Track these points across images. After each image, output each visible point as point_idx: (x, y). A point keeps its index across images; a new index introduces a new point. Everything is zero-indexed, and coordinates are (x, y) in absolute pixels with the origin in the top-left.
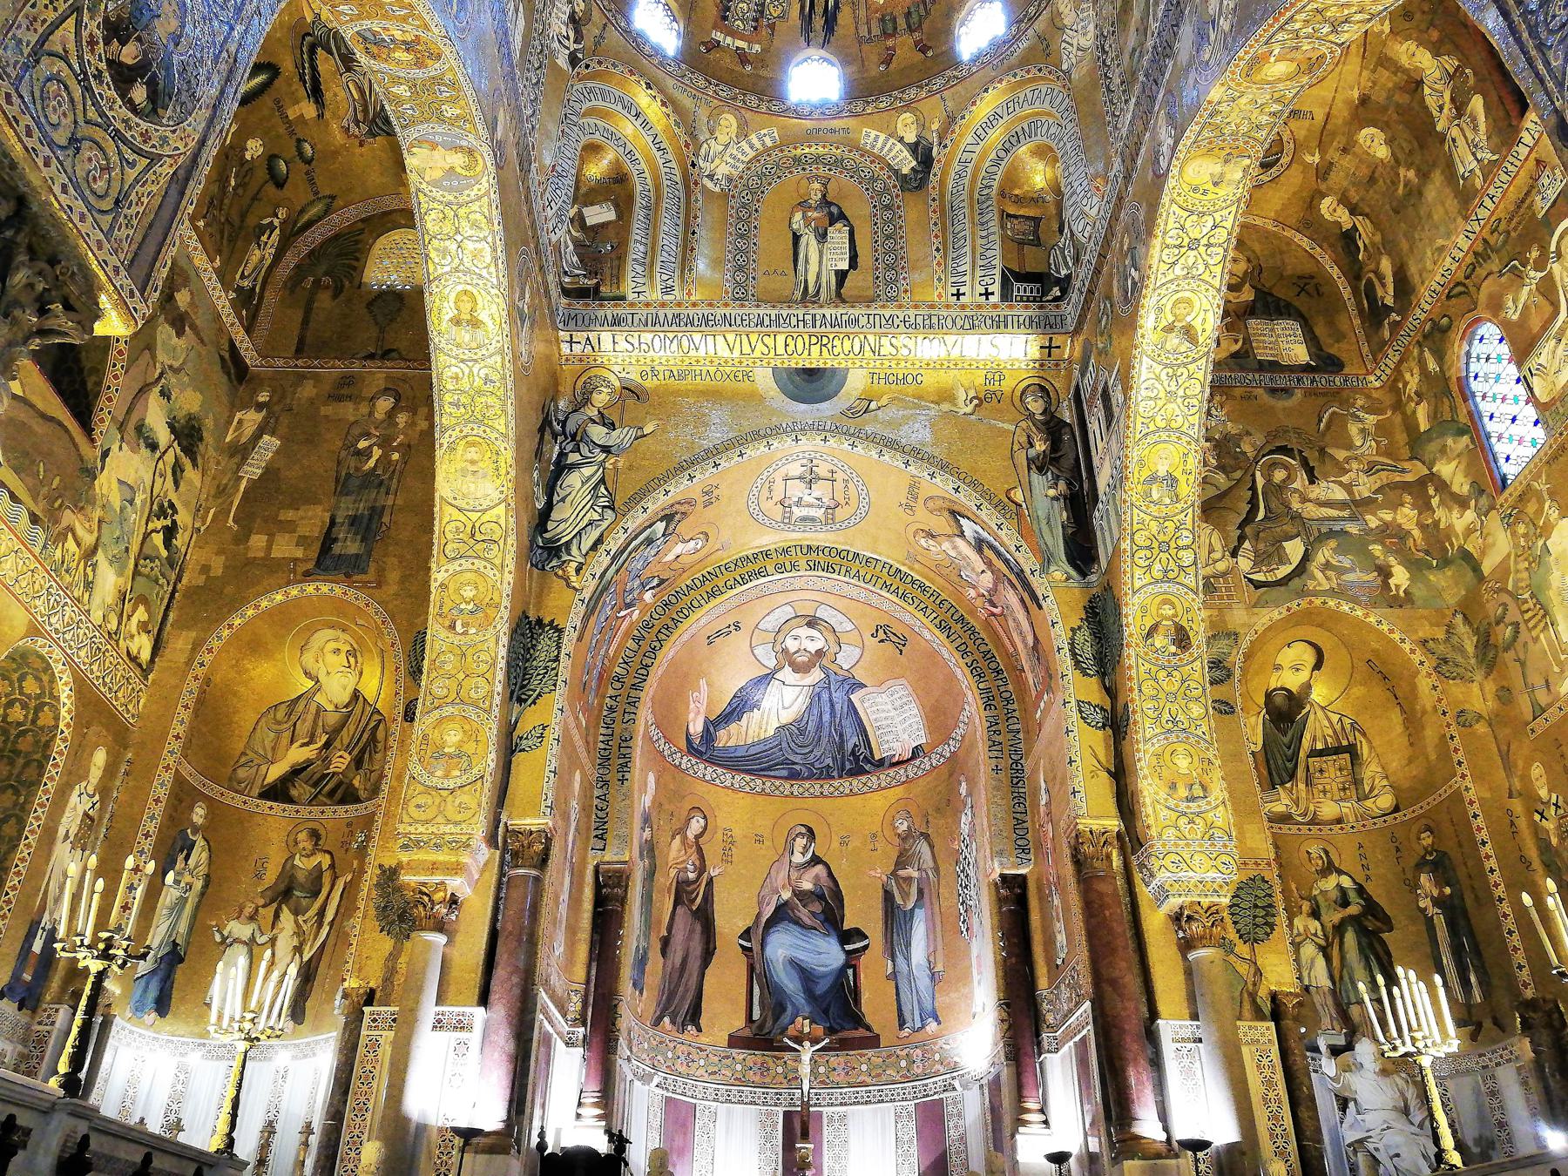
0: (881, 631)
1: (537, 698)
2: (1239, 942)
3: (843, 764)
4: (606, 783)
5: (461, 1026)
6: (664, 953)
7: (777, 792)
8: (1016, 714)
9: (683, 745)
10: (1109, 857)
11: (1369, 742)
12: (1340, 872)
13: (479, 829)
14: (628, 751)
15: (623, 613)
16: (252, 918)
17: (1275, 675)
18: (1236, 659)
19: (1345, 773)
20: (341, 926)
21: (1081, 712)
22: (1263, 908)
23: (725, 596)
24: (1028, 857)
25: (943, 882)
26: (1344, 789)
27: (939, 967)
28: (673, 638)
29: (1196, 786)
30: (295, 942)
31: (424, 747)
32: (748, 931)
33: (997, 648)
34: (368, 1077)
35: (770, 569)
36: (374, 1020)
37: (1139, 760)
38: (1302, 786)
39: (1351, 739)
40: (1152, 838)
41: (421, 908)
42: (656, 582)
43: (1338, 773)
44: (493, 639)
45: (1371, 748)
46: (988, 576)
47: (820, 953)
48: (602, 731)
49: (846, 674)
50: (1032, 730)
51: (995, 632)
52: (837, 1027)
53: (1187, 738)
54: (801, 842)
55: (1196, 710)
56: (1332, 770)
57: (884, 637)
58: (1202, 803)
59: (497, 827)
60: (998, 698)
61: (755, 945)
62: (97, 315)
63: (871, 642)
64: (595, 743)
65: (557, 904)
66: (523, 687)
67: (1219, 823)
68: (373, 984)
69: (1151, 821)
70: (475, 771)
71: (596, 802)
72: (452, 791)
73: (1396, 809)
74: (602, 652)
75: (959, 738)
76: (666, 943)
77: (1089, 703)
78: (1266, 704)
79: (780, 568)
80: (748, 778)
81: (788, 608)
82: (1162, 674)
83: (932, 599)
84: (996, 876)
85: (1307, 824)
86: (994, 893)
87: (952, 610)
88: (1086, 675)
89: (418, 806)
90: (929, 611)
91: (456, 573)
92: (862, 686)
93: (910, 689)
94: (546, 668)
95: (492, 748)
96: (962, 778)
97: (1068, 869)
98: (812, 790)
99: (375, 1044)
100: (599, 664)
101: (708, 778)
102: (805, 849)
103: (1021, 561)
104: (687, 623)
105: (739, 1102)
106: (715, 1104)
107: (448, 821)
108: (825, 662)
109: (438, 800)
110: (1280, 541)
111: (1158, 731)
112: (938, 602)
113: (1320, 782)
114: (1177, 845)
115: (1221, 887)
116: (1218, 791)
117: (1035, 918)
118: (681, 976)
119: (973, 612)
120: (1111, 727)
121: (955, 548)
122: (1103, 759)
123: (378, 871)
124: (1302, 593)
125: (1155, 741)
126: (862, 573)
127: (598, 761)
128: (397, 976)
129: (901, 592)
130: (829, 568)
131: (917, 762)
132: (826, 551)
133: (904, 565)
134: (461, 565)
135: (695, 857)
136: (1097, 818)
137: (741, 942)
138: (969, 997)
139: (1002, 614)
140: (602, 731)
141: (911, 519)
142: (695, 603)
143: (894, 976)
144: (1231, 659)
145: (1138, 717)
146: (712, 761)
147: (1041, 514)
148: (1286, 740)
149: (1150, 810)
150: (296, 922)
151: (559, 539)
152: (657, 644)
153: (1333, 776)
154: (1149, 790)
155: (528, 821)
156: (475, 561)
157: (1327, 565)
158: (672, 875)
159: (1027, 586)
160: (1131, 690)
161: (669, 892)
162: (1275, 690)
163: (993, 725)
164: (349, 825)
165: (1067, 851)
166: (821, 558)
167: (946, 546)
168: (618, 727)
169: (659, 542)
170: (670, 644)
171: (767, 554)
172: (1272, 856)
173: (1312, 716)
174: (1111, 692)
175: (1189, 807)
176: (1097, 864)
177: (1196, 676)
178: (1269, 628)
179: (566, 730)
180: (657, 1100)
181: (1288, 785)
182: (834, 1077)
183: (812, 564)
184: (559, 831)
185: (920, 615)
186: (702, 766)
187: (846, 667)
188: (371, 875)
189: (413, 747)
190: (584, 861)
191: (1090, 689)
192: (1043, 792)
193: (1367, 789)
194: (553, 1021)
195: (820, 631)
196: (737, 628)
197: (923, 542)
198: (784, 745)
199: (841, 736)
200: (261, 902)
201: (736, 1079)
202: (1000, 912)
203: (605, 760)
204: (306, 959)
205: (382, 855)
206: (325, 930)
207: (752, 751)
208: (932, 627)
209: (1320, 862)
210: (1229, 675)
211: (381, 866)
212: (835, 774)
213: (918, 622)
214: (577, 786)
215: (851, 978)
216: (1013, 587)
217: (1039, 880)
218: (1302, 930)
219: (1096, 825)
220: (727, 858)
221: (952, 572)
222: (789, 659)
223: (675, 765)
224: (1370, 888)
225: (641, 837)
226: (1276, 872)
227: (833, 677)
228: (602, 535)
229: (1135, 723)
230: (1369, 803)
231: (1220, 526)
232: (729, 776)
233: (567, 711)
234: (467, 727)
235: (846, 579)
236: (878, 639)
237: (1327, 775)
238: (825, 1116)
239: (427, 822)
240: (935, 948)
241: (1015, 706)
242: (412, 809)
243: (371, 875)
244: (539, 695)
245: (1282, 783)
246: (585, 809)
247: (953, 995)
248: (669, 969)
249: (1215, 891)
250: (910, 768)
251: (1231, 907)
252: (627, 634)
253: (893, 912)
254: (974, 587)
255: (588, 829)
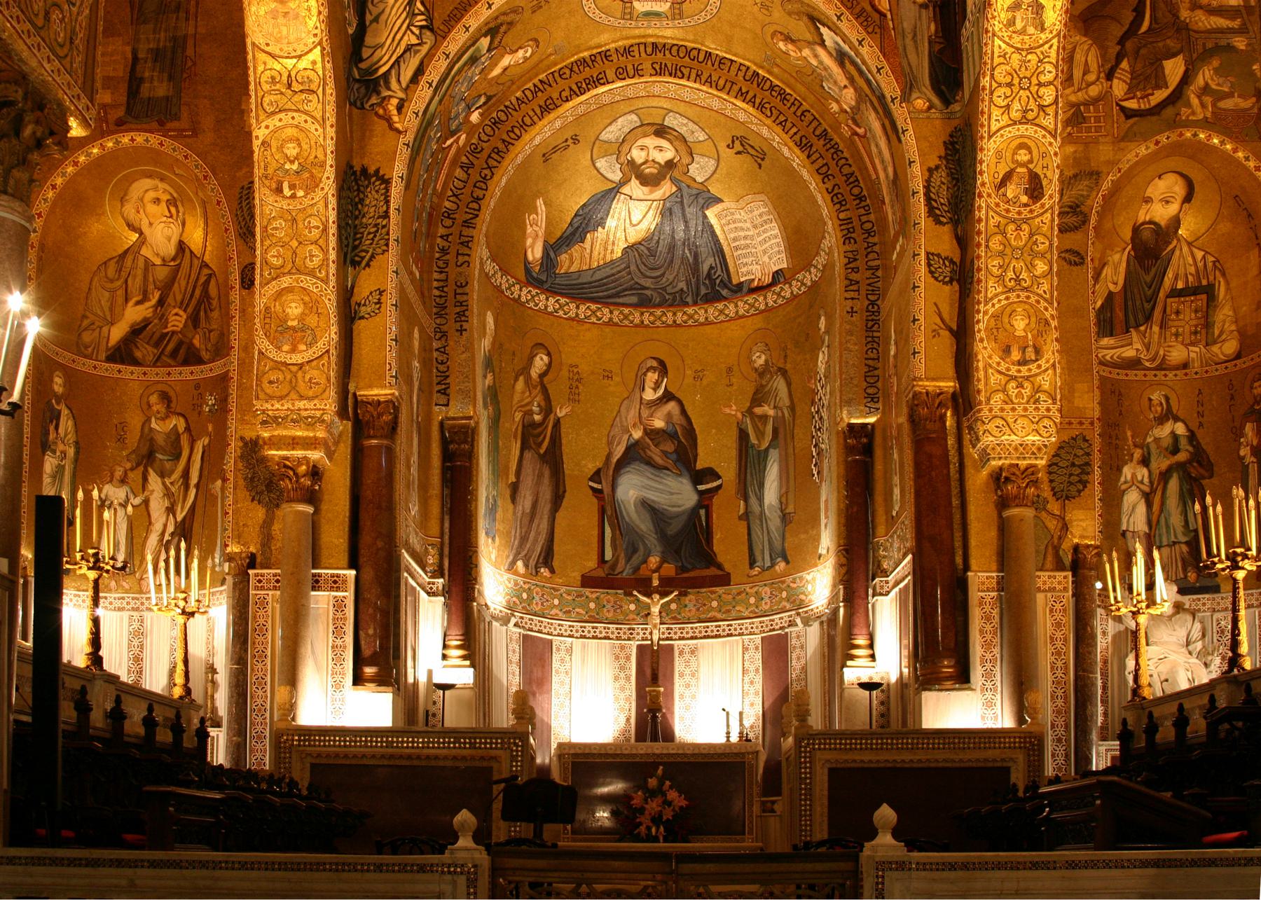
0: (737, 143)
1: (370, 260)
2: (1051, 499)
3: (698, 288)
4: (444, 335)
5: (336, 584)
6: (513, 499)
7: (626, 322)
8: (876, 248)
9: (521, 274)
10: (943, 417)
11: (1227, 283)
12: (1176, 419)
13: (328, 405)
14: (465, 298)
15: (449, 142)
16: (123, 481)
17: (1145, 207)
18: (1096, 203)
19: (1199, 315)
20: (208, 491)
21: (929, 265)
22: (1079, 466)
23: (561, 110)
24: (877, 406)
25: (797, 422)
26: (1196, 333)
27: (790, 509)
28: (505, 163)
29: (1030, 349)
30: (167, 504)
31: (268, 320)
32: (598, 472)
33: (860, 170)
34: (262, 630)
35: (610, 74)
36: (260, 581)
37: (978, 322)
38: (1156, 329)
39: (1211, 278)
40: (980, 403)
41: (288, 481)
42: (483, 100)
43: (1193, 315)
44: (322, 203)
45: (1228, 289)
46: (851, 90)
47: (672, 494)
48: (436, 276)
49: (700, 187)
50: (891, 270)
51: (858, 152)
52: (689, 566)
53: (1028, 297)
54: (652, 377)
55: (1041, 267)
56: (1188, 310)
57: (741, 149)
58: (1033, 366)
59: (346, 398)
60: (858, 228)
61: (605, 486)
62: (68, 129)
63: (727, 154)
64: (430, 289)
65: (408, 467)
66: (355, 247)
67: (1046, 386)
68: (252, 549)
69: (981, 386)
70: (320, 344)
71: (435, 354)
72: (301, 366)
73: (1238, 356)
74: (430, 191)
75: (820, 267)
76: (515, 489)
77: (939, 255)
78: (1132, 239)
79: (621, 74)
80: (593, 307)
81: (634, 117)
82: (1011, 227)
83: (793, 109)
84: (843, 425)
85: (1156, 369)
86: (842, 441)
87: (815, 123)
88: (938, 222)
89: (271, 382)
90: (789, 125)
91: (277, 129)
92: (719, 200)
93: (771, 208)
94: (376, 225)
95: (333, 320)
96: (822, 312)
97: (906, 427)
98: (664, 319)
99: (263, 603)
100: (428, 205)
101: (550, 309)
102: (657, 386)
103: (883, 85)
104: (519, 144)
105: (594, 638)
106: (570, 640)
107: (302, 397)
108: (676, 174)
109: (288, 377)
110: (1161, 60)
111: (999, 290)
112: (799, 113)
113: (1175, 324)
114: (1002, 410)
115: (1039, 449)
116: (1051, 352)
117: (879, 467)
118: (531, 520)
119: (837, 128)
120: (958, 281)
121: (816, 56)
122: (946, 316)
123: (241, 444)
124: (1175, 124)
125: (995, 301)
126: (714, 78)
127: (435, 310)
128: (274, 542)
129: (758, 101)
130: (676, 72)
131: (777, 289)
132: (674, 49)
133: (762, 67)
134: (280, 120)
135: (539, 398)
136: (933, 379)
137: (591, 484)
138: (817, 539)
139: (864, 136)
140: (436, 276)
141: (768, 20)
142: (528, 121)
143: (746, 516)
144: (1089, 202)
145: (982, 275)
146: (552, 291)
147: (907, 26)
148: (1148, 279)
149: (981, 374)
150: (164, 484)
151: (377, 69)
152: (487, 172)
153: (1187, 318)
154: (985, 352)
155: (375, 392)
156: (295, 114)
157: (1206, 89)
158: (517, 419)
159: (888, 114)
160: (979, 245)
161: (515, 437)
162: (1143, 224)
163: (851, 260)
164: (197, 387)
165: (905, 410)
166: (668, 60)
167: (806, 52)
168: (452, 271)
169: (483, 59)
170: (501, 172)
171: (606, 55)
172: (1097, 414)
173: (1177, 253)
174: (964, 241)
175: (1019, 371)
176: (929, 426)
177: (1045, 229)
178: (1137, 163)
179: (402, 290)
180: (515, 637)
181: (1142, 328)
182: (685, 614)
183: (657, 68)
184: (404, 397)
185: (779, 129)
186: (543, 297)
187: (699, 179)
188: (234, 448)
189: (257, 320)
190: (429, 417)
191: (944, 243)
192: (893, 342)
193: (1217, 332)
194: (415, 576)
195: (669, 140)
196: (575, 140)
197: (781, 45)
198: (633, 268)
199: (696, 256)
200: (128, 465)
201: (590, 616)
202: (846, 461)
203: (442, 309)
204: (179, 518)
205: (236, 429)
206: (193, 492)
207: (598, 276)
208: (792, 144)
209: (1159, 409)
210: (1085, 221)
211: (242, 438)
212: (689, 300)
213: (777, 139)
214: (416, 344)
215: (703, 518)
216: (875, 109)
217: (884, 430)
218: (1129, 477)
219: (931, 386)
220: (574, 397)
221: (814, 79)
222: (634, 171)
223: (514, 299)
224: (1200, 434)
225: (484, 385)
226: (1098, 430)
227: (685, 190)
228: (422, 63)
229: (979, 281)
230: (1215, 349)
231: (1100, 43)
232: (572, 306)
233: (403, 272)
234: (307, 299)
235: (697, 85)
236: (734, 151)
237: (1181, 317)
238: (676, 648)
239: (281, 398)
240: (788, 488)
241: (876, 240)
242: (265, 385)
243: (234, 448)
244: (372, 257)
245: (1137, 326)
246: (426, 363)
247: (803, 536)
248: (519, 515)
249: (1033, 453)
250: (769, 295)
251: (1050, 466)
252: (455, 162)
253: (747, 451)
254: (838, 102)
255: (431, 384)
